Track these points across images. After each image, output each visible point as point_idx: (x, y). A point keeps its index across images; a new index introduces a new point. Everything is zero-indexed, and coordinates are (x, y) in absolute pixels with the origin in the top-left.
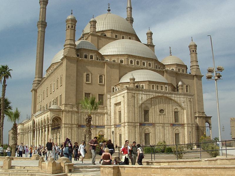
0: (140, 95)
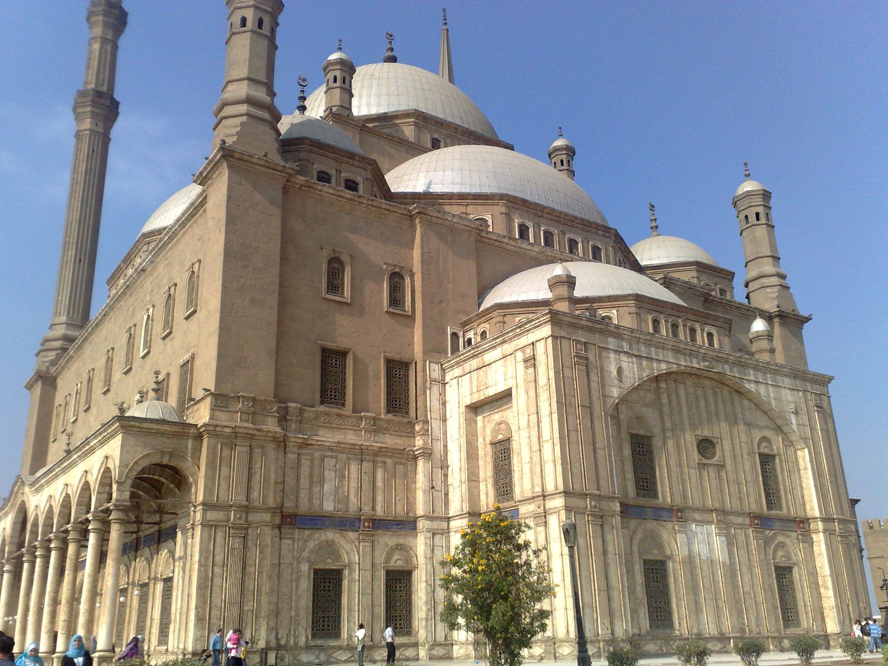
0: (612, 355)
